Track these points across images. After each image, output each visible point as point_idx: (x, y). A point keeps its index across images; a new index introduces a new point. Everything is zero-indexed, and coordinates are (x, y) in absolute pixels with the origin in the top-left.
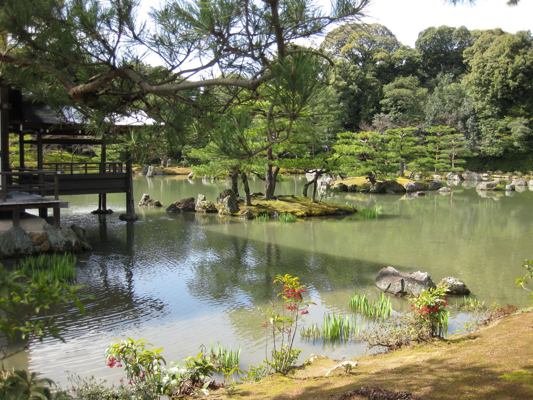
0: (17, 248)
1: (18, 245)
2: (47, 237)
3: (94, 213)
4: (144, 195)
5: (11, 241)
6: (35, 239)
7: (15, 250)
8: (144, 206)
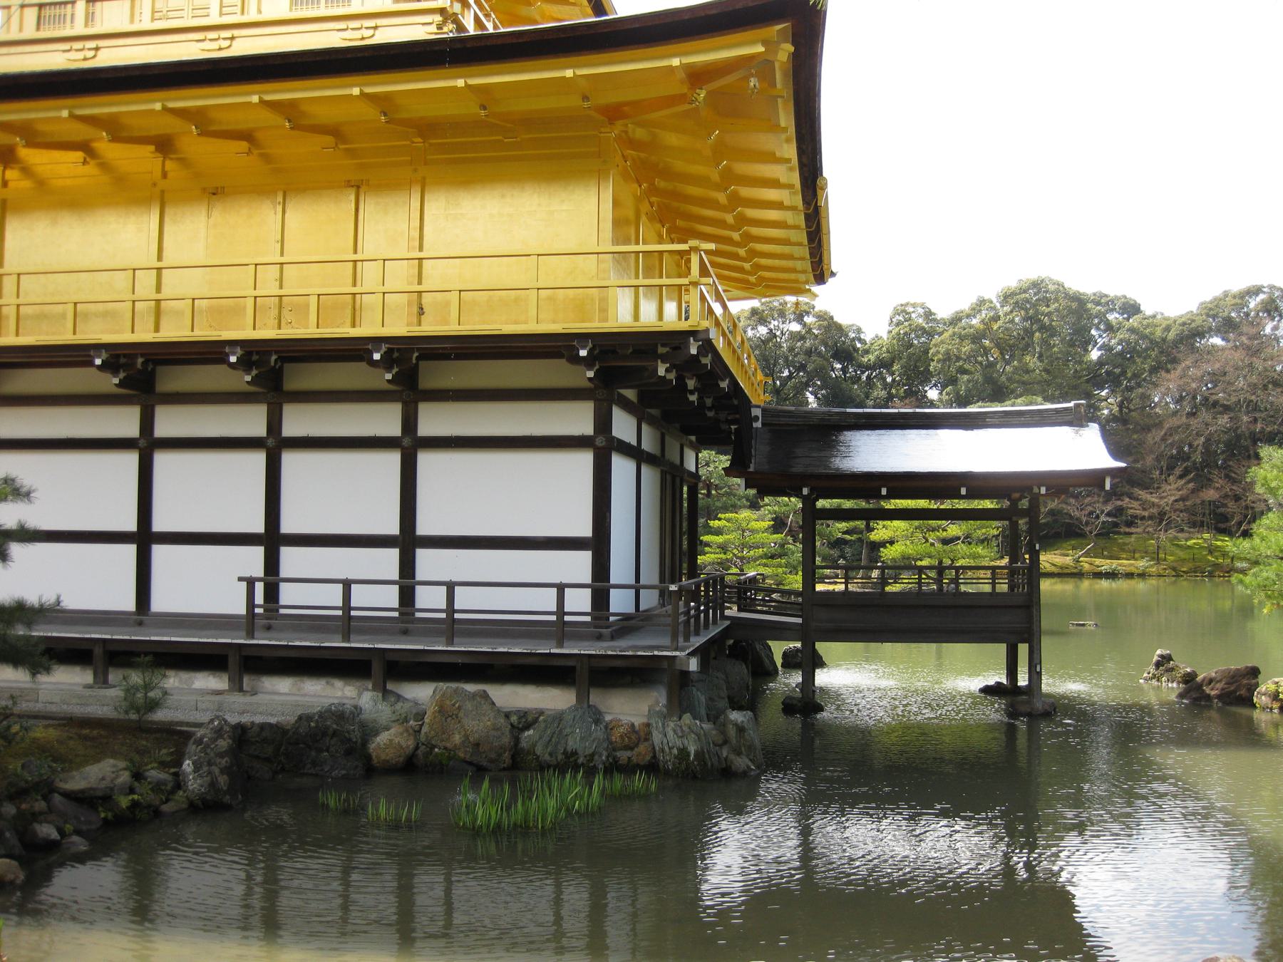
0: (569, 749)
1: (572, 744)
2: (649, 734)
3: (987, 690)
4: (1159, 652)
5: (561, 731)
6: (615, 737)
7: (565, 753)
8: (1154, 682)
